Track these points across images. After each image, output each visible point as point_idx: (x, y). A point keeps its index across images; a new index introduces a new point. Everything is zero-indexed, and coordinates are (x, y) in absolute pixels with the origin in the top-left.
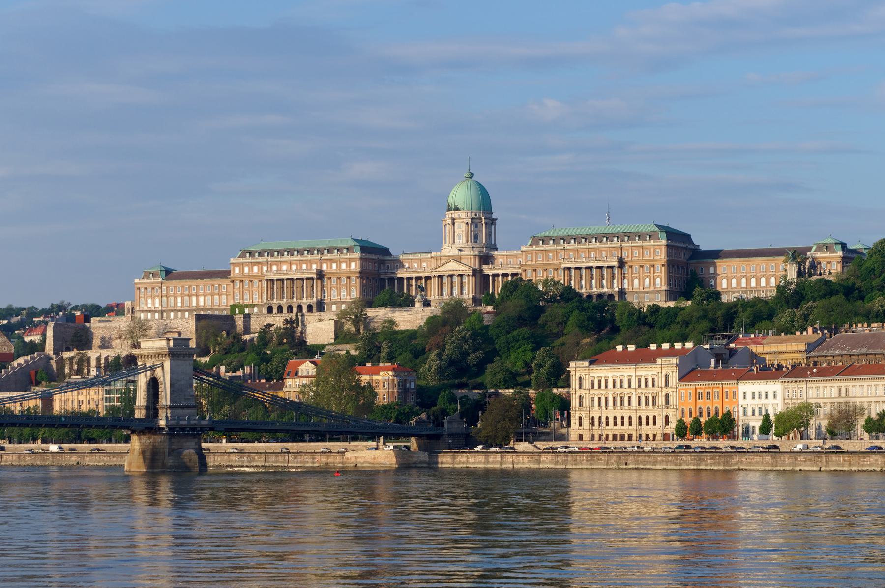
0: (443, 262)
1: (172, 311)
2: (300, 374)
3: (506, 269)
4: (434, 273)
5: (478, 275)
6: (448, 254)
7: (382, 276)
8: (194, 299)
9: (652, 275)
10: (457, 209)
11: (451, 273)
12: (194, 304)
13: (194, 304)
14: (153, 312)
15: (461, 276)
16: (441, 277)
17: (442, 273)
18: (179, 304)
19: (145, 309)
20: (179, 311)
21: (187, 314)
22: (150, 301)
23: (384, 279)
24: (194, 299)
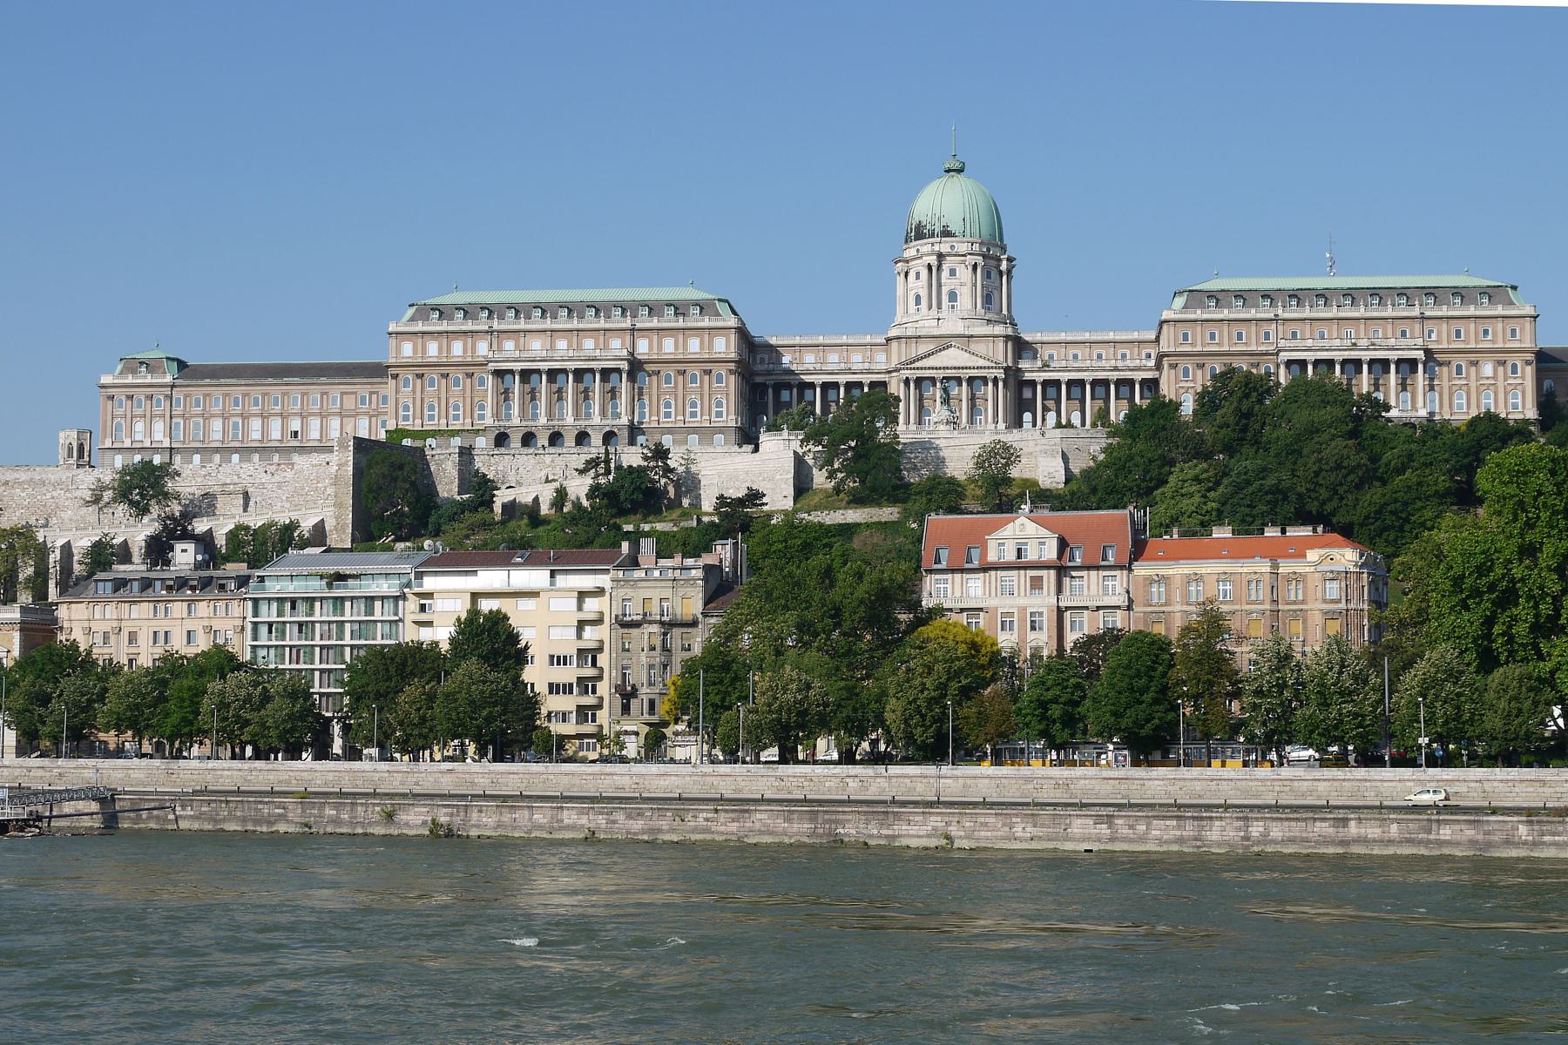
0: (923, 348)
1: (197, 450)
4: (906, 373)
5: (1011, 381)
7: (759, 380)
8: (256, 424)
9: (1501, 384)
10: (946, 233)
11: (950, 373)
13: (256, 435)
16: (919, 381)
17: (927, 373)
19: (127, 444)
20: (217, 450)
23: (764, 386)
24: (256, 424)
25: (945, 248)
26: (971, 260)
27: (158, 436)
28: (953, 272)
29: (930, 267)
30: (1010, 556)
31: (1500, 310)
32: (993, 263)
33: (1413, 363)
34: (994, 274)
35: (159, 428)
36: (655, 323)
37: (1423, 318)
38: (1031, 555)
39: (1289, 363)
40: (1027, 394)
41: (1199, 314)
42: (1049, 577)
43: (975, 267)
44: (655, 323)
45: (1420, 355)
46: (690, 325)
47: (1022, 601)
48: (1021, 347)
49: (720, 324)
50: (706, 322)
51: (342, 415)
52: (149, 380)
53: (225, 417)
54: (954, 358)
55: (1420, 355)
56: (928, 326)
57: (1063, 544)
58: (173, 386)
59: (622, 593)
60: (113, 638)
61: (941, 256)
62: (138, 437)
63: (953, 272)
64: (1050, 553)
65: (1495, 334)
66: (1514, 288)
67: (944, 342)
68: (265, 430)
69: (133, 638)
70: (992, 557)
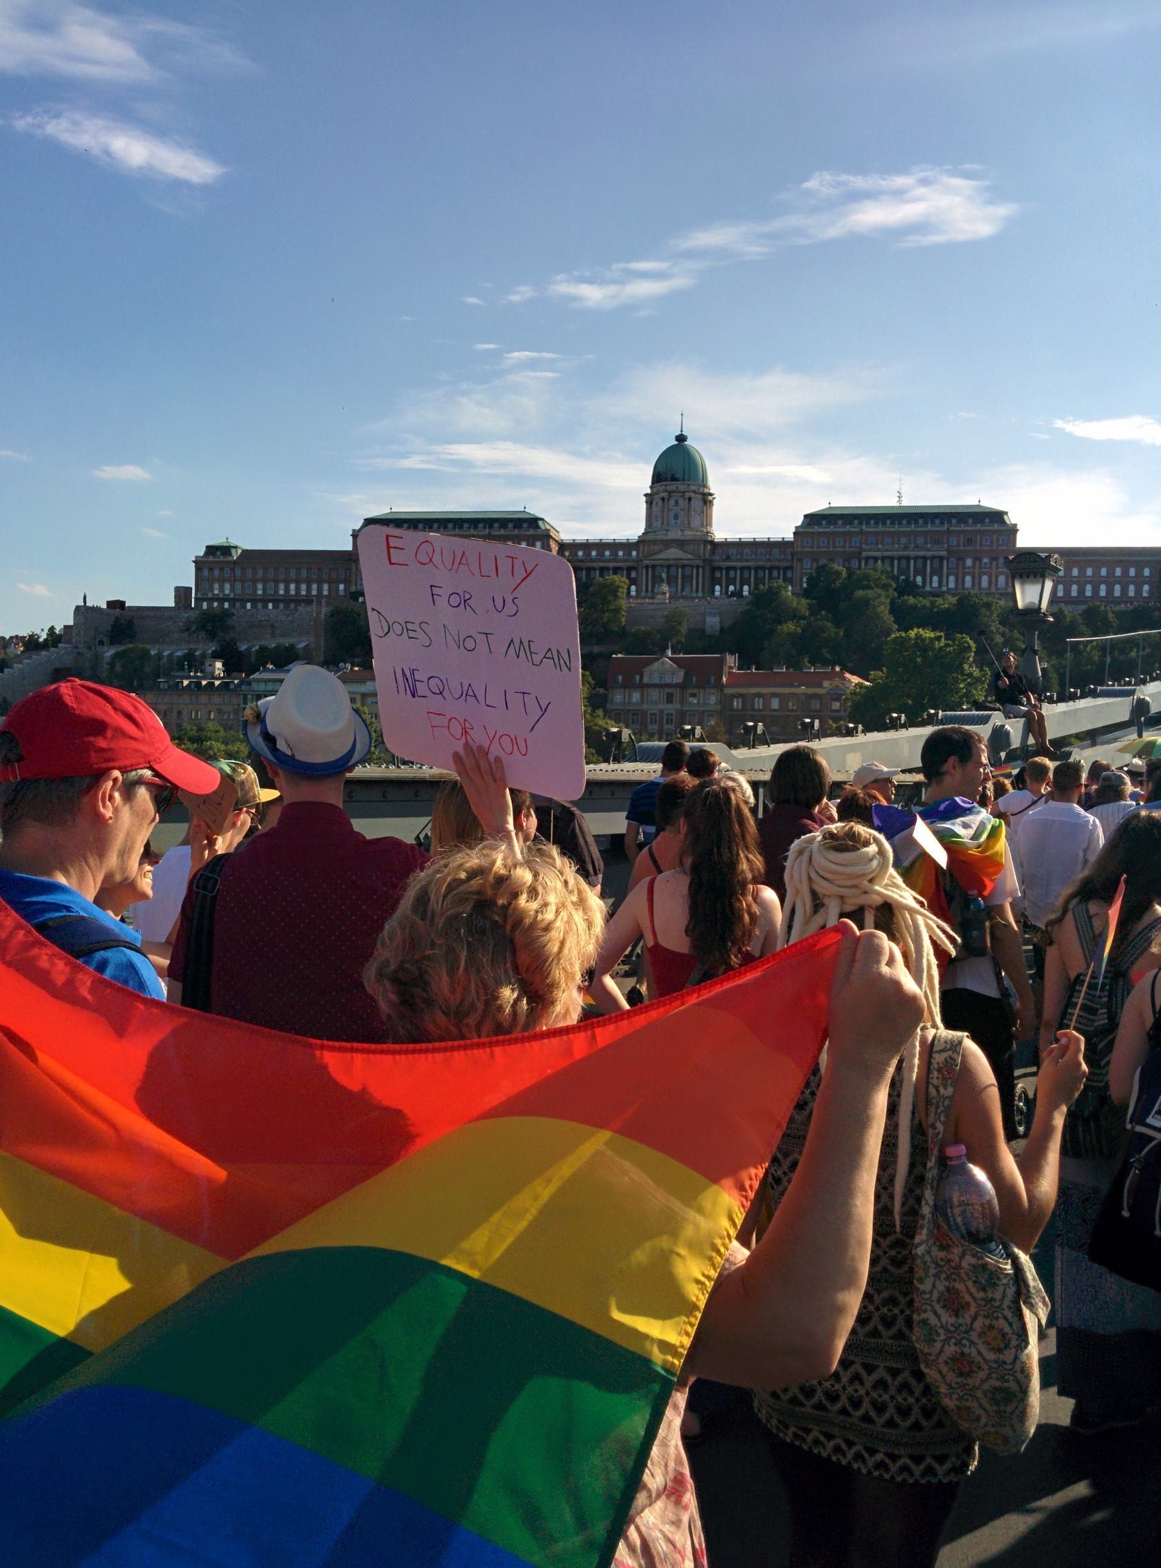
2: (646, 680)
3: (747, 561)
5: (707, 568)
8: (282, 586)
10: (674, 479)
12: (282, 592)
14: (222, 601)
15: (683, 567)
16: (654, 567)
17: (659, 562)
18: (260, 592)
19: (210, 595)
20: (260, 600)
21: (270, 606)
22: (216, 586)
24: (282, 586)
25: (674, 488)
26: (687, 495)
27: (227, 592)
28: (677, 503)
29: (663, 499)
30: (656, 681)
32: (700, 497)
33: (941, 558)
34: (701, 503)
35: (227, 586)
36: (502, 532)
37: (949, 532)
38: (668, 681)
39: (867, 559)
40: (718, 575)
41: (816, 529)
42: (677, 693)
43: (690, 499)
44: (502, 532)
45: (944, 553)
46: (522, 532)
47: (662, 706)
49: (539, 532)
50: (531, 532)
51: (329, 582)
52: (222, 559)
53: (264, 581)
54: (673, 553)
58: (235, 562)
62: (216, 592)
63: (677, 503)
64: (679, 678)
65: (992, 543)
66: (1006, 513)
67: (668, 544)
68: (287, 589)
70: (646, 680)
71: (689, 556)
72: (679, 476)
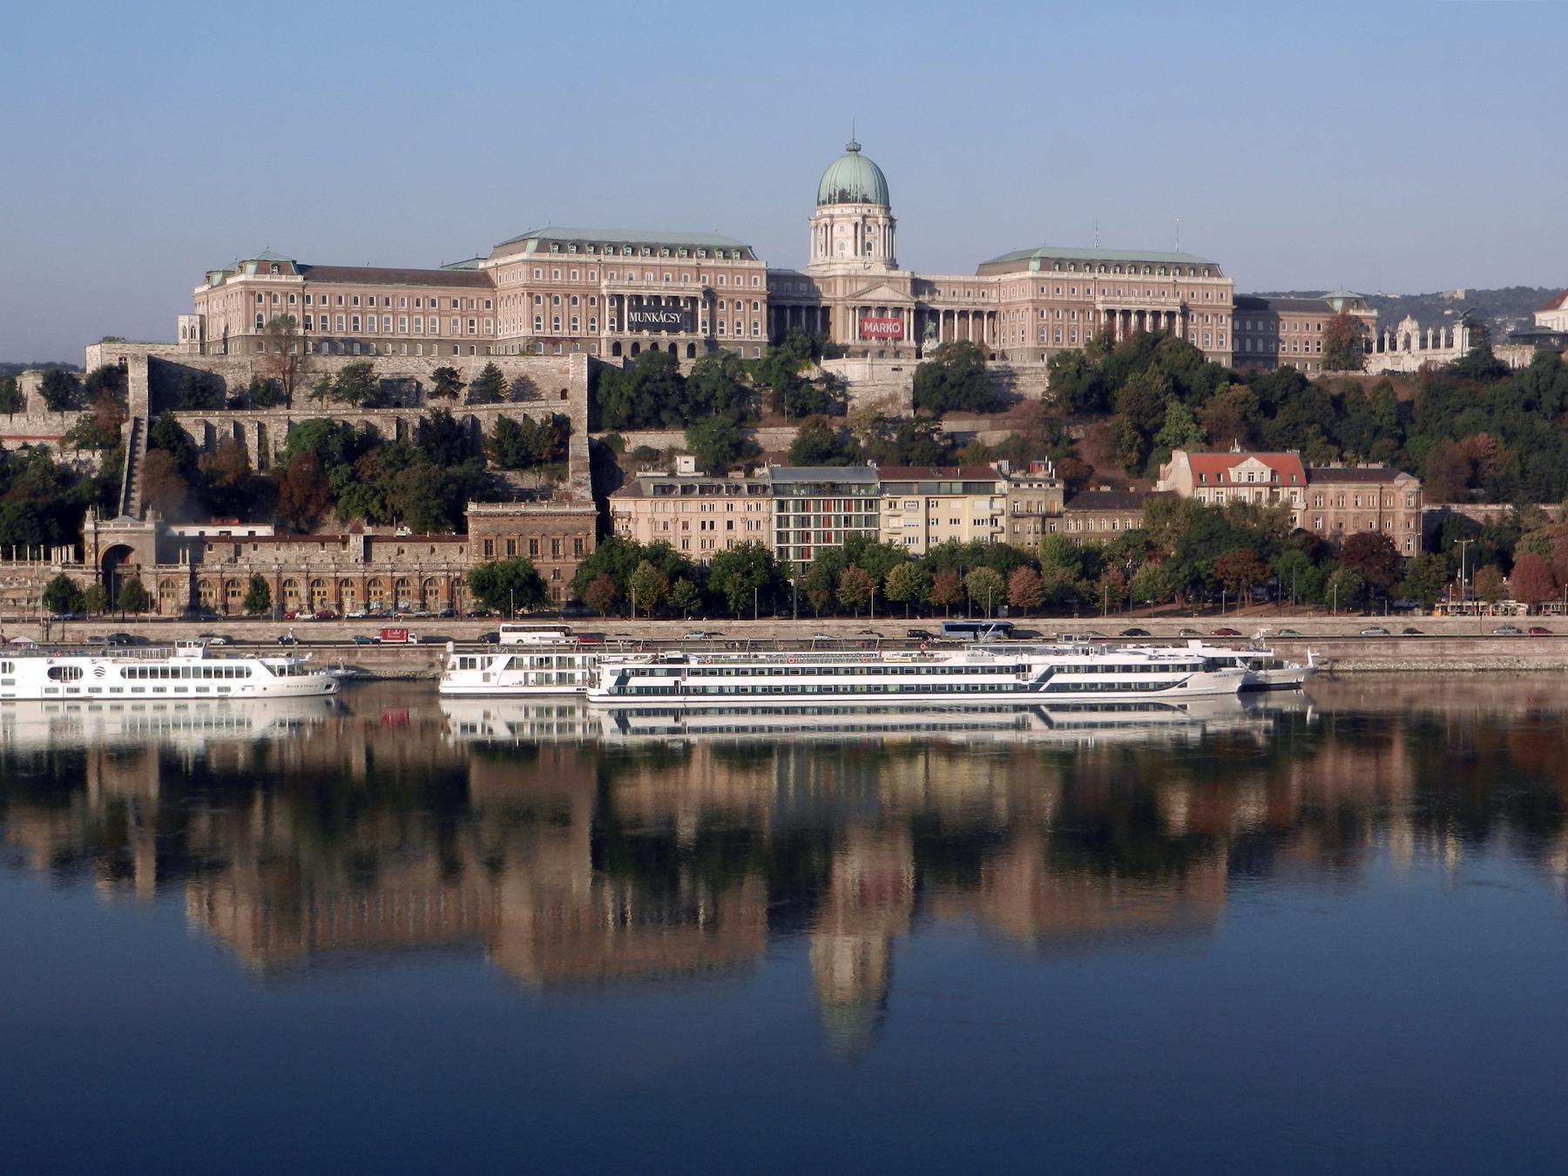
0: (861, 286)
4: (855, 303)
6: (868, 273)
10: (865, 200)
25: (865, 211)
29: (856, 225)
30: (1244, 479)
31: (1215, 280)
38: (1257, 479)
48: (918, 286)
54: (884, 294)
55: (1178, 309)
56: (857, 266)
57: (1273, 473)
59: (1014, 497)
60: (671, 526)
61: (864, 217)
64: (1267, 478)
69: (685, 526)
70: (1234, 479)
71: (901, 297)
72: (871, 196)
